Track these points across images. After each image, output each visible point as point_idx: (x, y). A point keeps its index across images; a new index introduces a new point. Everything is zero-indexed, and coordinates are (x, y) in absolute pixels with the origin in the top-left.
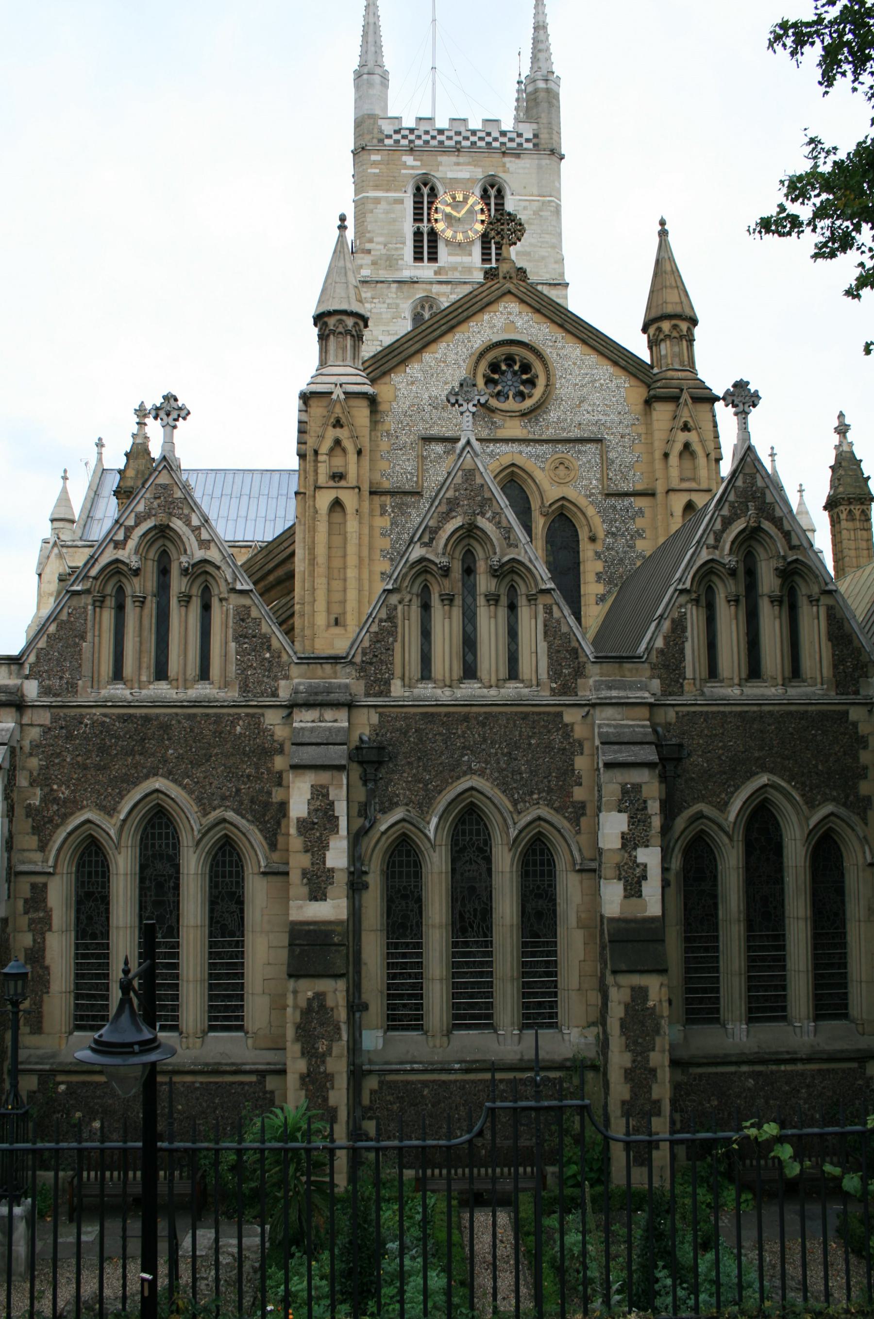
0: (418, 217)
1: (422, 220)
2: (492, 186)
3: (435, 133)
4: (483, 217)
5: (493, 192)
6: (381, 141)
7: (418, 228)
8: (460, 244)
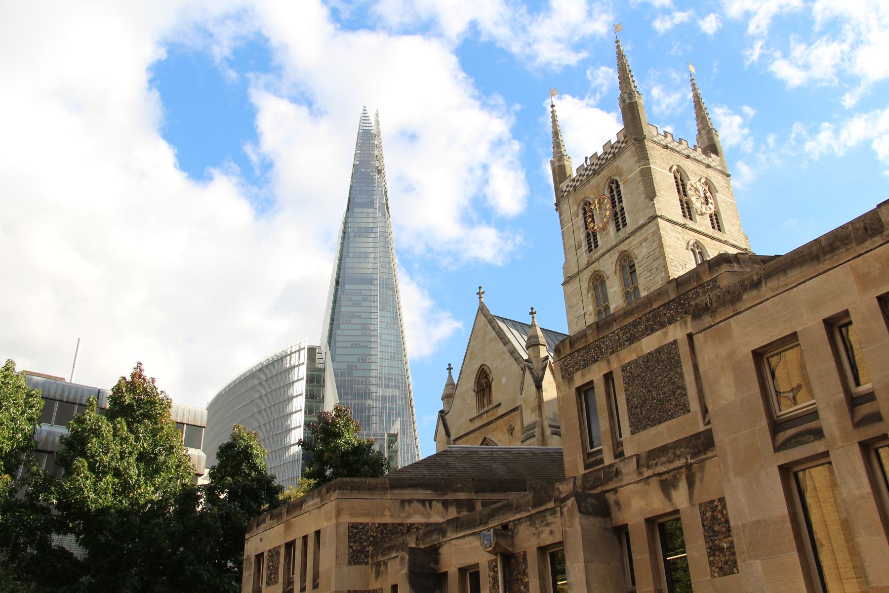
2: (613, 183)
5: (614, 186)
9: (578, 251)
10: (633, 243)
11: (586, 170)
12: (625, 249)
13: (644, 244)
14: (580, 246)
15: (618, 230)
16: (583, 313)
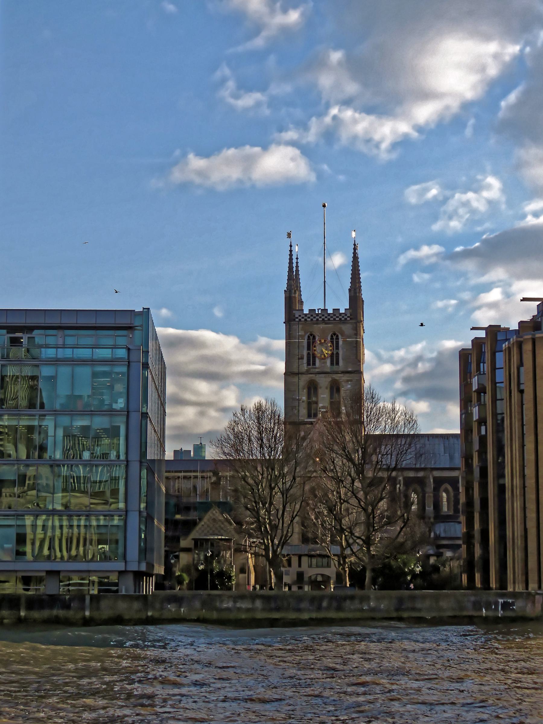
0: (309, 349)
1: (310, 350)
2: (335, 335)
3: (315, 316)
4: (331, 348)
5: (335, 337)
6: (294, 320)
7: (309, 353)
8: (323, 359)
9: (300, 360)
10: (343, 378)
11: (318, 315)
12: (337, 378)
13: (349, 382)
14: (302, 358)
15: (332, 364)
16: (298, 398)
